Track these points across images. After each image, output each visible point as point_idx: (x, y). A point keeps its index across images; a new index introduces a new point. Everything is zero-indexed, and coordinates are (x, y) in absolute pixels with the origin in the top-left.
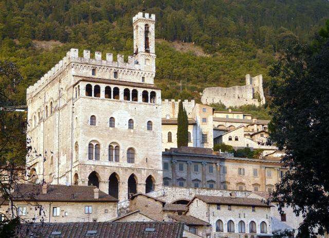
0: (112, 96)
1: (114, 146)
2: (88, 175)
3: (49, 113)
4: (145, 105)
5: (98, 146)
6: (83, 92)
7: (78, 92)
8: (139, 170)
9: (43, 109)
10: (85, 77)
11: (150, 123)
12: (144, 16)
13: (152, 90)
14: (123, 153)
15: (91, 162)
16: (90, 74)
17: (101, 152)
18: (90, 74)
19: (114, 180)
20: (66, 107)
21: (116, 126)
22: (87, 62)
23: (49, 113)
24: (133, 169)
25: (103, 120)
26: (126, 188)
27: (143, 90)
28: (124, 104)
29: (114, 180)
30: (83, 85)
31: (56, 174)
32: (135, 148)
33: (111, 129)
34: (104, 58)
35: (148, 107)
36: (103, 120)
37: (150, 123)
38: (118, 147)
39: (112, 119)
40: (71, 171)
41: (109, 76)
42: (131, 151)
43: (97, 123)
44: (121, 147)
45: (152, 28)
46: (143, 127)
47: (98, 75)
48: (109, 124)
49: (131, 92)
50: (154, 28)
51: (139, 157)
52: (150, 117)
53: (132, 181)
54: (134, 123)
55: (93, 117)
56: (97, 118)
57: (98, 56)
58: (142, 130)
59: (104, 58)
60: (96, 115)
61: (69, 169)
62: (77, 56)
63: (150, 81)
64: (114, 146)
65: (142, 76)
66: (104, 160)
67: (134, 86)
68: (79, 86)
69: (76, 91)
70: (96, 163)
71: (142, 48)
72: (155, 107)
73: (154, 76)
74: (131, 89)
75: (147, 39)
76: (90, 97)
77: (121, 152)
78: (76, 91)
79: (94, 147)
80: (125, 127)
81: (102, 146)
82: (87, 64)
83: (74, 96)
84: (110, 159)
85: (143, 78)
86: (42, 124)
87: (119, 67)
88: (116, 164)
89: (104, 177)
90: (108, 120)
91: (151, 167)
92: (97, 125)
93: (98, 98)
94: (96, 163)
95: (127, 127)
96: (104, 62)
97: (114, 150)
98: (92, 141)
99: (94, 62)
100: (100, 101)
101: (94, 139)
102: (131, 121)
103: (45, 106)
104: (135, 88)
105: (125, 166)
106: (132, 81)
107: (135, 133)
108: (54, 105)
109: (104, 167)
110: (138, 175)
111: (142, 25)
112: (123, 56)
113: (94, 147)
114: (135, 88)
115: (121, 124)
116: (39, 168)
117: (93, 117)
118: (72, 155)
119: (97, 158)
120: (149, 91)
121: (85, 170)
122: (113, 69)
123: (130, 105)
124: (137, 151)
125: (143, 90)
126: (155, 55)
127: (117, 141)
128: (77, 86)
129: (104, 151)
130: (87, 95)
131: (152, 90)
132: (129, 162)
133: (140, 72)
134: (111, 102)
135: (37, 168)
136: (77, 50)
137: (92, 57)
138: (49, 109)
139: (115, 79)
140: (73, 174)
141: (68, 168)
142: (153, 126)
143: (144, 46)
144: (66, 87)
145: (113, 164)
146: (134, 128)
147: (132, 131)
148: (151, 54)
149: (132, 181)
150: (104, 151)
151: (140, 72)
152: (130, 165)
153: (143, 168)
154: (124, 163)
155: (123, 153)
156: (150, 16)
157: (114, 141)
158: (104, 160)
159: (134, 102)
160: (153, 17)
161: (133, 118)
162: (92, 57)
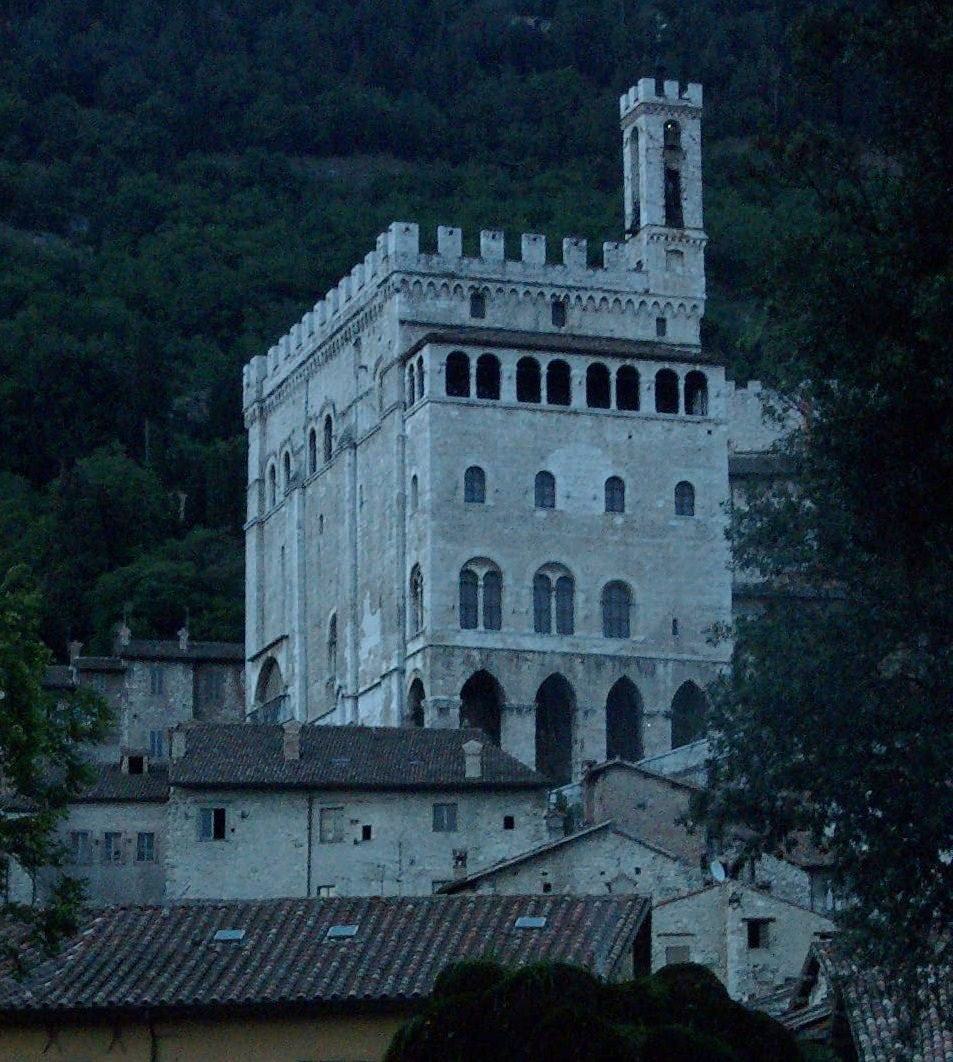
0: (544, 393)
1: (554, 577)
2: (460, 685)
3: (320, 456)
4: (666, 424)
5: (495, 577)
6: (435, 383)
7: (416, 381)
8: (648, 666)
9: (302, 439)
10: (444, 326)
11: (685, 493)
12: (659, 90)
14: (587, 604)
15: (470, 638)
16: (462, 314)
17: (507, 601)
18: (462, 314)
19: (555, 703)
20: (379, 438)
21: (560, 503)
22: (451, 268)
23: (320, 456)
24: (624, 661)
25: (509, 483)
26: (600, 730)
27: (657, 367)
28: (588, 421)
29: (555, 703)
30: (433, 359)
31: (349, 678)
32: (634, 584)
33: (542, 514)
34: (513, 253)
35: (678, 430)
37: (685, 491)
38: (568, 581)
39: (545, 480)
40: (402, 672)
41: (532, 319)
42: (615, 594)
43: (489, 493)
44: (581, 582)
45: (691, 133)
46: (660, 504)
47: (495, 317)
48: (532, 496)
49: (613, 377)
50: (697, 134)
51: (647, 616)
52: (686, 466)
53: (624, 704)
54: (627, 491)
55: (475, 475)
56: (489, 477)
57: (492, 244)
58: (653, 516)
59: (513, 253)
60: (484, 466)
61: (394, 664)
62: (417, 250)
63: (685, 332)
64: (554, 577)
65: (657, 313)
66: (518, 632)
67: (625, 356)
68: (421, 361)
69: (412, 380)
70: (492, 641)
71: (652, 213)
72: (702, 430)
73: (701, 311)
74: (614, 367)
75: (672, 177)
76: (464, 400)
77: (579, 598)
78: (412, 380)
79: (481, 583)
80: (594, 504)
81: (508, 580)
82: (452, 276)
83: (407, 400)
85: (661, 323)
86: (296, 494)
87: (570, 282)
88: (563, 645)
89: (521, 687)
90: (531, 482)
91: (694, 652)
92: (489, 502)
93: (491, 402)
94: (492, 641)
95: (600, 507)
96: (513, 267)
97: (554, 591)
98: (470, 561)
99: (475, 267)
100: (499, 415)
101: (478, 552)
102: (615, 485)
103: (308, 431)
104: (628, 362)
105: (595, 651)
106: (616, 336)
107: (629, 526)
108: (338, 429)
109: (517, 655)
110: (643, 685)
112: (584, 243)
113: (481, 583)
114: (628, 362)
116: (290, 659)
117: (475, 475)
118: (402, 611)
119: (494, 622)
120: (682, 370)
121: (448, 665)
122: (548, 293)
123: (614, 426)
124: (639, 596)
125: (657, 367)
126: (703, 235)
127: (564, 560)
128: (414, 361)
129: (518, 596)
130: (450, 392)
132: (609, 634)
133: (650, 301)
134: (540, 417)
135: (281, 658)
136: (415, 228)
137: (471, 249)
138: (320, 442)
139: (555, 329)
140: (409, 681)
141: (387, 658)
142: (699, 501)
143: (662, 202)
144: (377, 365)
145: (552, 643)
146: (627, 511)
147: (619, 520)
148: (687, 233)
149: (624, 704)
150: (518, 596)
151: (650, 301)
152: (612, 647)
153: (663, 656)
154: (589, 638)
155: (587, 604)
156: (683, 89)
157: (553, 558)
158: (518, 632)
159: (626, 413)
160: (695, 92)
161: (623, 475)
162: (471, 249)
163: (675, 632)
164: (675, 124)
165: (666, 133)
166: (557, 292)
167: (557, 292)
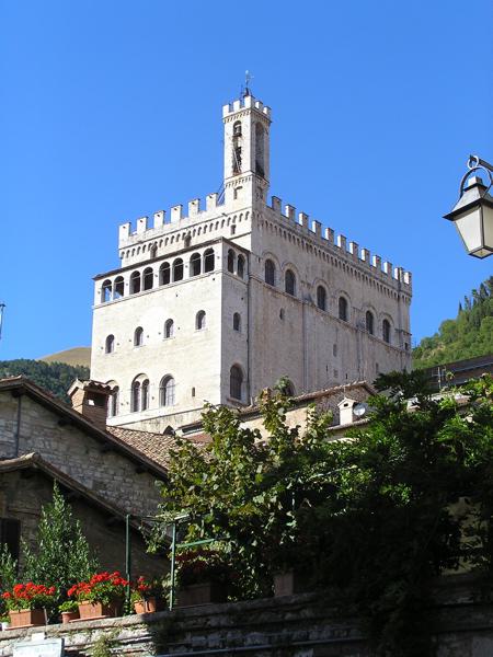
11: (201, 315)
13: (205, 249)
25: (124, 338)
33: (137, 349)
36: (124, 338)
39: (139, 331)
45: (246, 121)
57: (158, 220)
59: (166, 220)
71: (228, 171)
84: (135, 409)
99: (151, 234)
102: (169, 323)
107: (175, 344)
111: (229, 129)
115: (153, 331)
131: (205, 249)
142: (207, 318)
163: (194, 395)
164: (239, 122)
165: (235, 129)
166: (185, 231)
167: (185, 231)
